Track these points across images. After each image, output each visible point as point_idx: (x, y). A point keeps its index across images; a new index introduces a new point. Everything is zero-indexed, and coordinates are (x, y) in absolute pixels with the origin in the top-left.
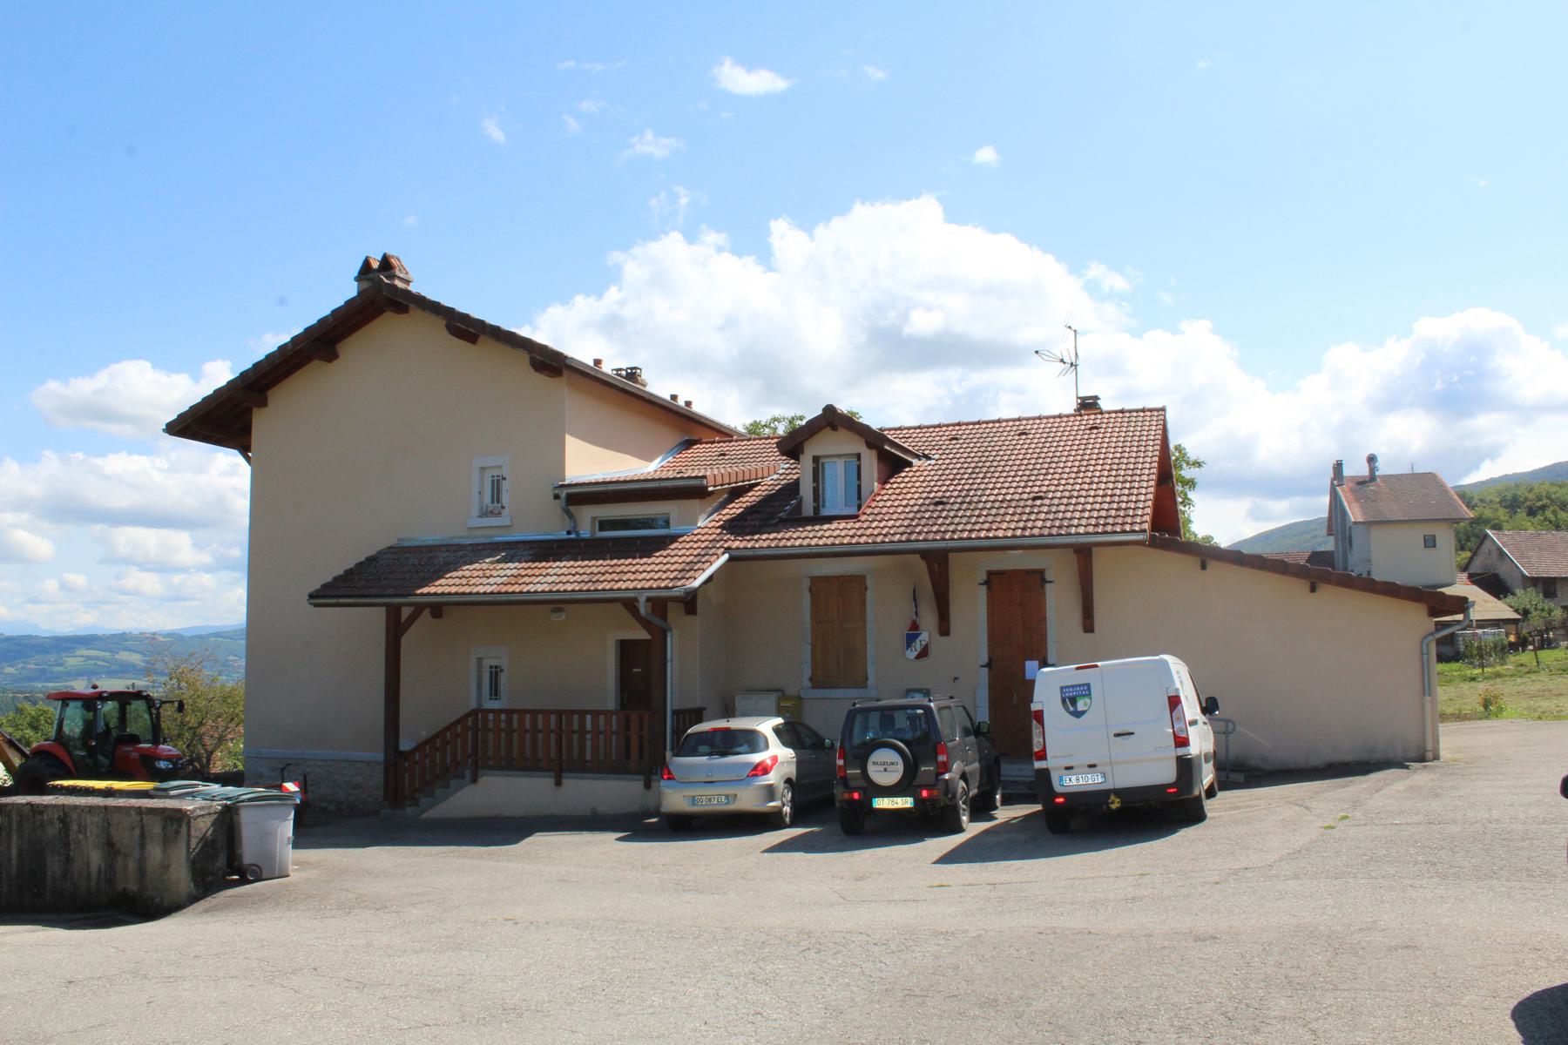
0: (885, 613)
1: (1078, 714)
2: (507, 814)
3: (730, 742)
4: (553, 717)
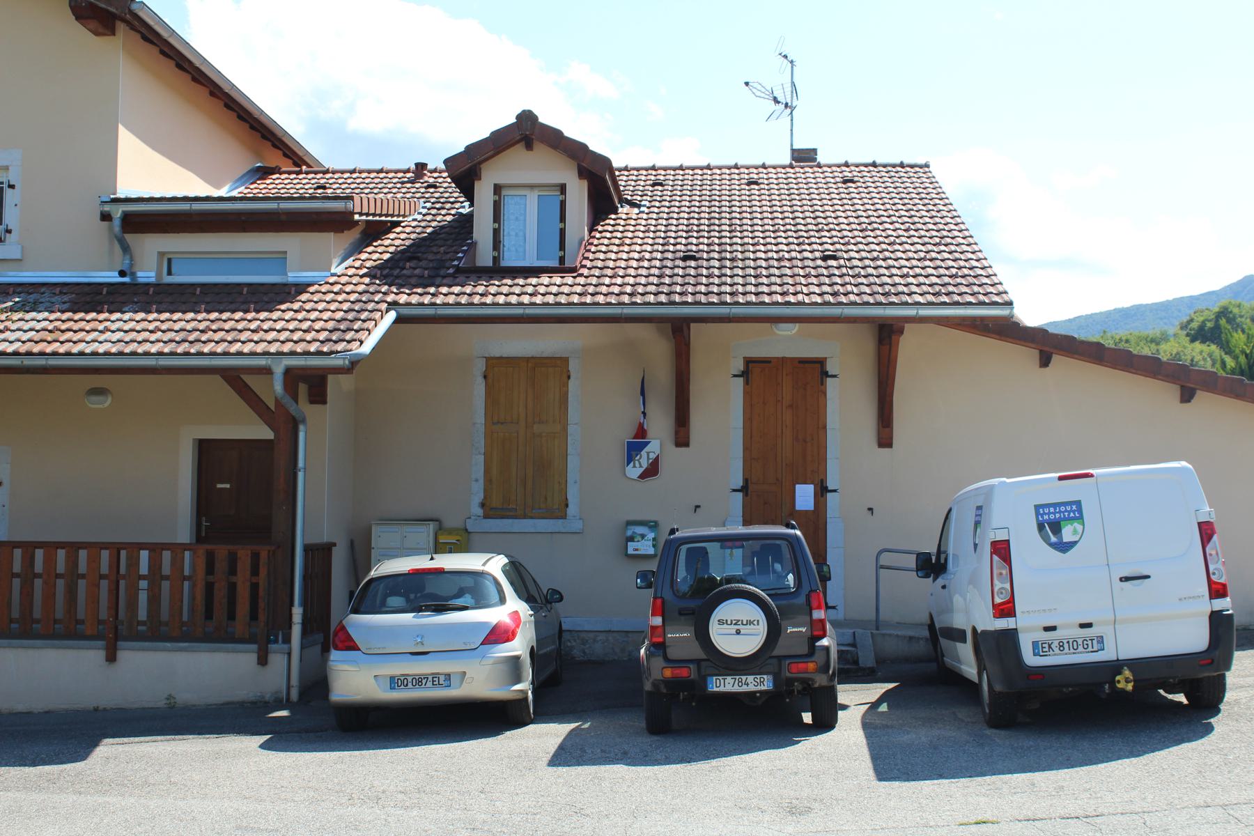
0: (594, 416)
1: (1064, 547)
2: (20, 708)
3: (426, 593)
4: (105, 554)
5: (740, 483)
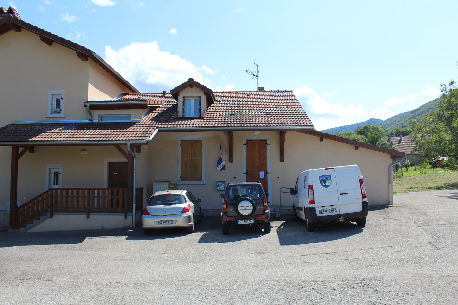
0: (209, 155)
1: (326, 186)
2: (66, 229)
3: (167, 200)
4: (86, 191)
5: (246, 171)
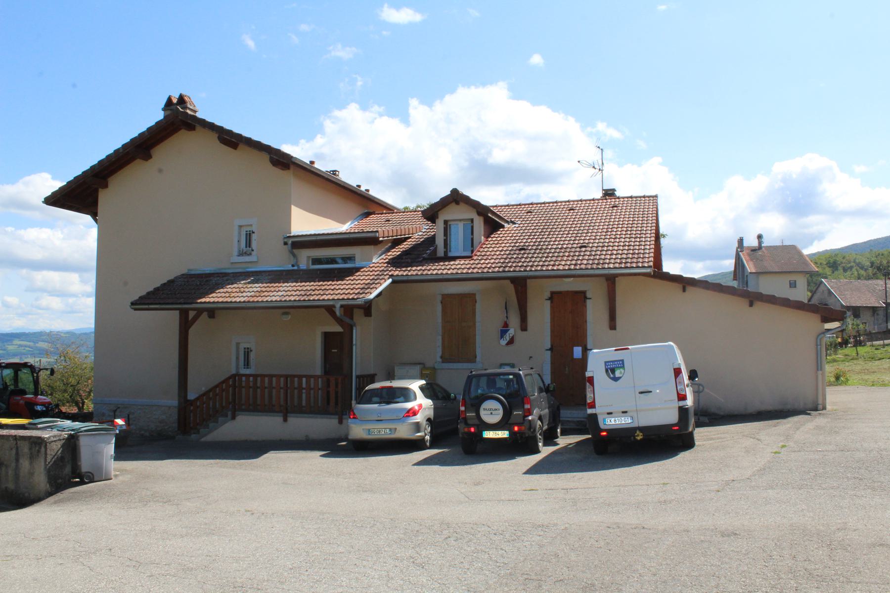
0: (487, 317)
1: (616, 379)
2: (254, 438)
4: (282, 379)
5: (549, 346)
